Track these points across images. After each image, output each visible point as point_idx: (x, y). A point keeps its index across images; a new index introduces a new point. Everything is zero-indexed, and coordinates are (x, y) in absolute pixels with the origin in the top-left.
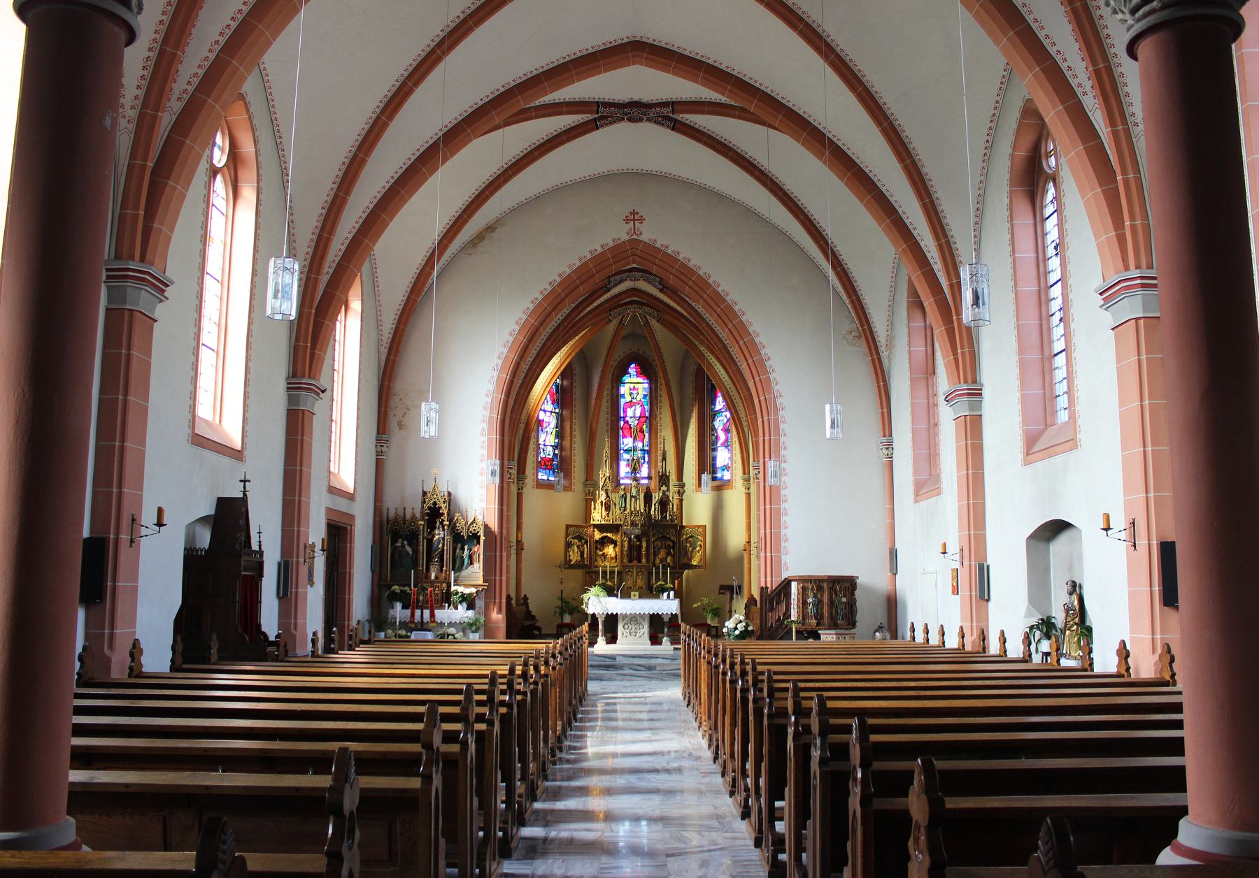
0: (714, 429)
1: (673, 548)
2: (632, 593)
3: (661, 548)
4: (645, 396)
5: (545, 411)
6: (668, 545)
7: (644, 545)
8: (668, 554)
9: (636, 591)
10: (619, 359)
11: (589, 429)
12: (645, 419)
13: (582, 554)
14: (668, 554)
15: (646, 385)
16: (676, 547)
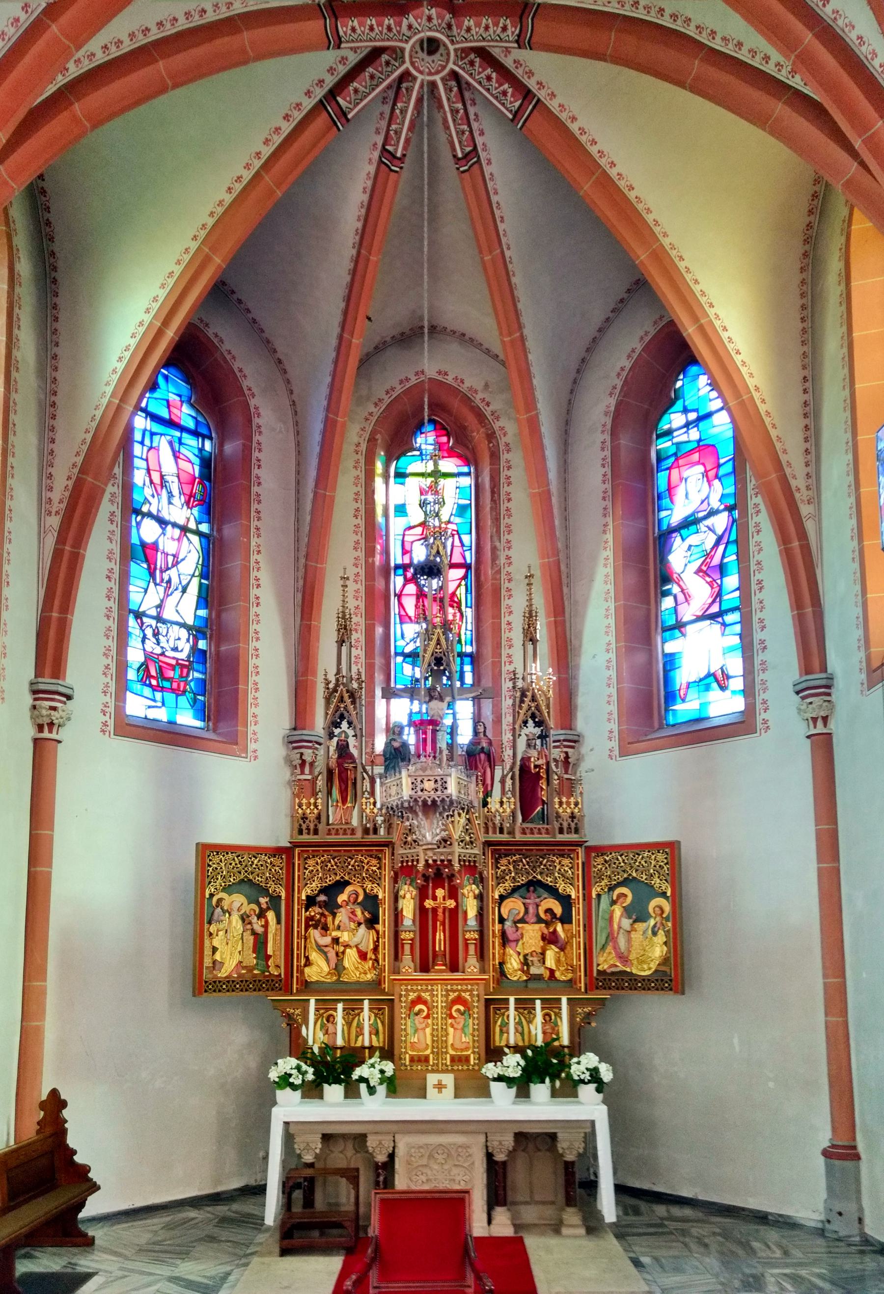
0: (666, 577)
1: (566, 919)
2: (432, 1079)
3: (523, 921)
4: (462, 510)
5: (162, 522)
6: (549, 911)
7: (471, 908)
8: (550, 939)
9: (446, 1071)
10: (387, 400)
11: (301, 583)
12: (461, 572)
13: (260, 943)
14: (550, 939)
15: (466, 481)
16: (578, 913)
